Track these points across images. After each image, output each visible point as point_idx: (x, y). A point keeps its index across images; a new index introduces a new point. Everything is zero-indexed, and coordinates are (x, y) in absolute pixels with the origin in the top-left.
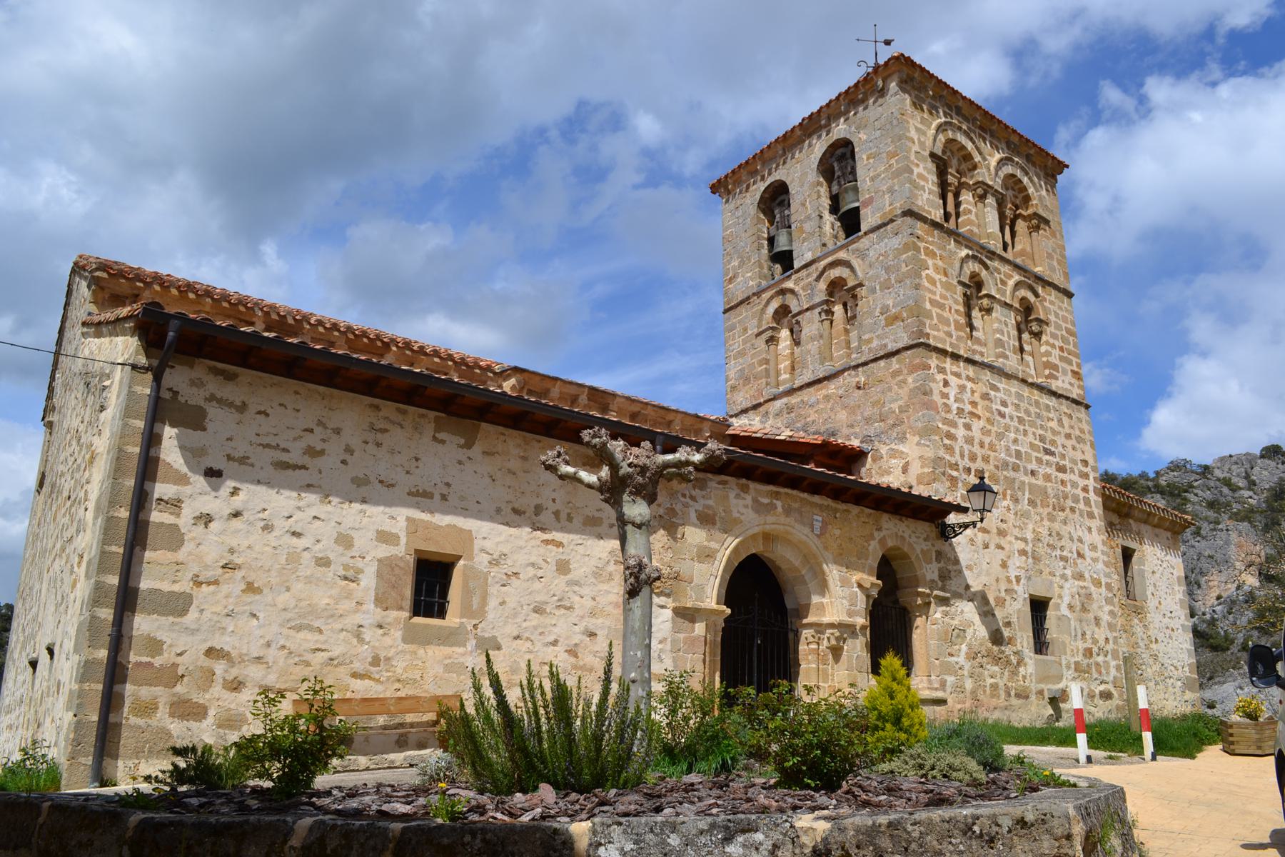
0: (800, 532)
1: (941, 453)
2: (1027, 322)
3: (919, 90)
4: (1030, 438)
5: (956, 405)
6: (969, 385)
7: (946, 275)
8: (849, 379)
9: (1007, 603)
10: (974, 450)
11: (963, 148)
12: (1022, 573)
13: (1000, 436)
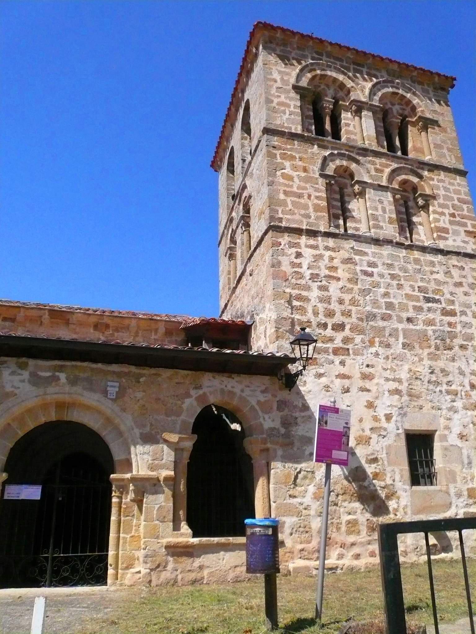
0: (91, 399)
1: (287, 313)
2: (415, 199)
3: (285, 45)
4: (408, 290)
5: (310, 271)
6: (328, 254)
7: (305, 170)
9: (373, 442)
10: (332, 307)
11: (335, 80)
12: (395, 412)
13: (364, 292)
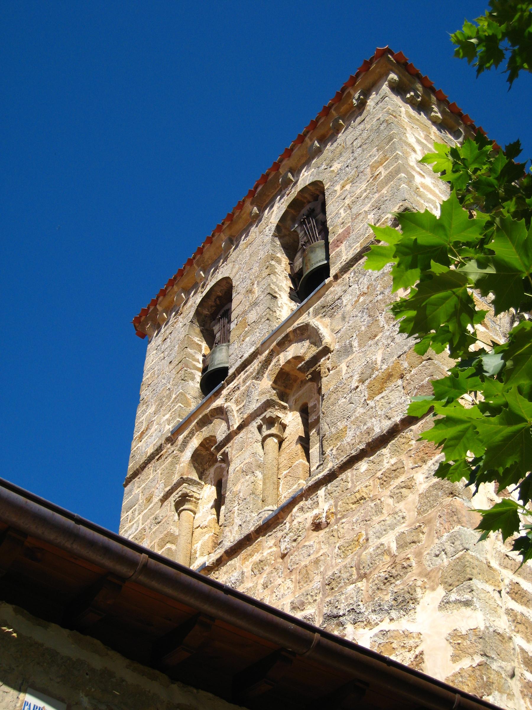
8: (302, 517)
